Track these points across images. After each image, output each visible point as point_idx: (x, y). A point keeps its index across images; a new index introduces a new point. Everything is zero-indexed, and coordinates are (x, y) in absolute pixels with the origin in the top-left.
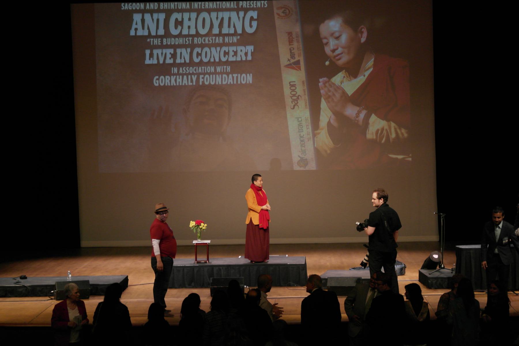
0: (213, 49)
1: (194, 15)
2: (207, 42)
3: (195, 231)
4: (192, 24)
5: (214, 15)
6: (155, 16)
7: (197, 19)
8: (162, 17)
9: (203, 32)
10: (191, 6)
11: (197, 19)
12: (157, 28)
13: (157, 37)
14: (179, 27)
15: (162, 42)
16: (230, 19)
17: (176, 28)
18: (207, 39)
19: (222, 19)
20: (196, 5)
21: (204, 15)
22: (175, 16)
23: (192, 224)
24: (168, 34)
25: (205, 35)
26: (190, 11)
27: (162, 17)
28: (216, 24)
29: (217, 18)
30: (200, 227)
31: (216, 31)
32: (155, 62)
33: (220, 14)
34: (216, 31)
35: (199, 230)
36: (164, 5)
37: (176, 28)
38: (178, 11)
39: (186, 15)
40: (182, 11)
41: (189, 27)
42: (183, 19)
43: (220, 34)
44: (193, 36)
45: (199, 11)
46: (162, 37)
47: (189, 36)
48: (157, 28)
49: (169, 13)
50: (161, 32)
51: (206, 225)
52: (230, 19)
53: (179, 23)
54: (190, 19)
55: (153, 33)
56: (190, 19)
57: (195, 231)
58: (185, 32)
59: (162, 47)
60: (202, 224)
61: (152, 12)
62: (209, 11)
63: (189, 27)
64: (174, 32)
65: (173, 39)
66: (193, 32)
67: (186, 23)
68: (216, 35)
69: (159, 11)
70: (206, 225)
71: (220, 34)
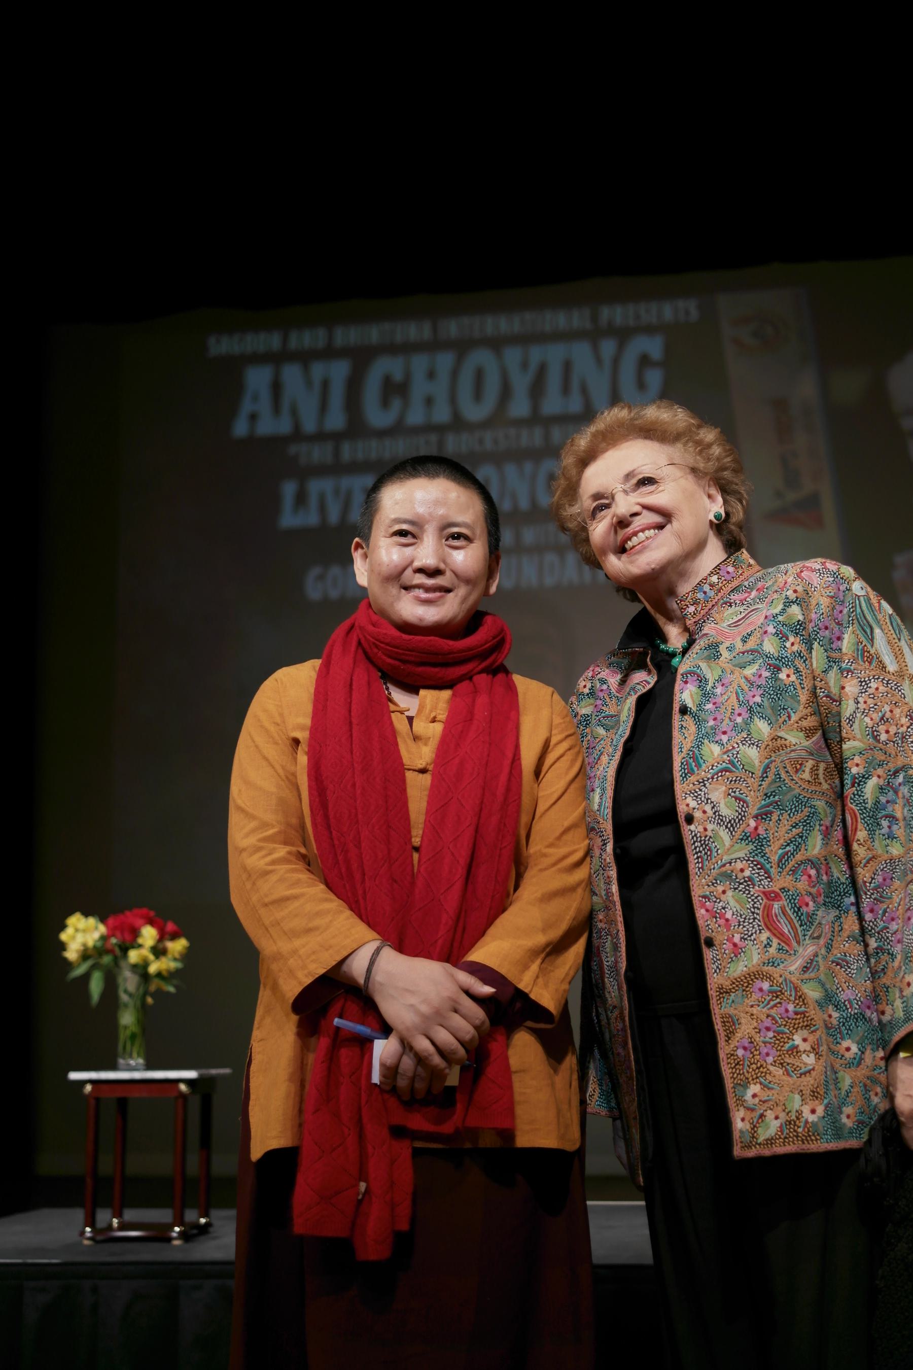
0: (510, 470)
1: (445, 361)
2: (488, 445)
3: (96, 986)
4: (440, 388)
5: (513, 355)
6: (318, 370)
7: (455, 374)
8: (339, 370)
9: (474, 412)
10: (435, 330)
11: (455, 374)
12: (324, 407)
13: (321, 436)
14: (396, 404)
15: (337, 453)
16: (567, 367)
17: (385, 403)
18: (488, 437)
19: (542, 370)
20: (452, 328)
21: (482, 357)
22: (385, 367)
23: (81, 933)
24: (356, 427)
25: (486, 424)
26: (434, 346)
27: (339, 370)
28: (521, 384)
29: (525, 365)
30: (134, 956)
31: (520, 407)
32: (312, 519)
33: (536, 354)
34: (520, 407)
35: (129, 982)
36: (347, 335)
37: (385, 403)
38: (392, 349)
39: (419, 363)
40: (407, 349)
41: (429, 401)
42: (408, 376)
43: (536, 419)
44: (440, 429)
45: (462, 347)
46: (337, 437)
47: (429, 428)
48: (324, 407)
49: (361, 358)
50: (336, 420)
51: (178, 946)
52: (567, 367)
53: (395, 390)
54: (431, 375)
55: (309, 426)
56: (431, 375)
57: (96, 986)
58: (416, 416)
59: (337, 469)
60: (149, 935)
61: (305, 358)
62: (496, 344)
63: (429, 401)
64: (377, 416)
65: (374, 443)
66: (442, 414)
67: (419, 388)
68: (519, 423)
69: (329, 353)
70: (178, 946)
71: (536, 419)
